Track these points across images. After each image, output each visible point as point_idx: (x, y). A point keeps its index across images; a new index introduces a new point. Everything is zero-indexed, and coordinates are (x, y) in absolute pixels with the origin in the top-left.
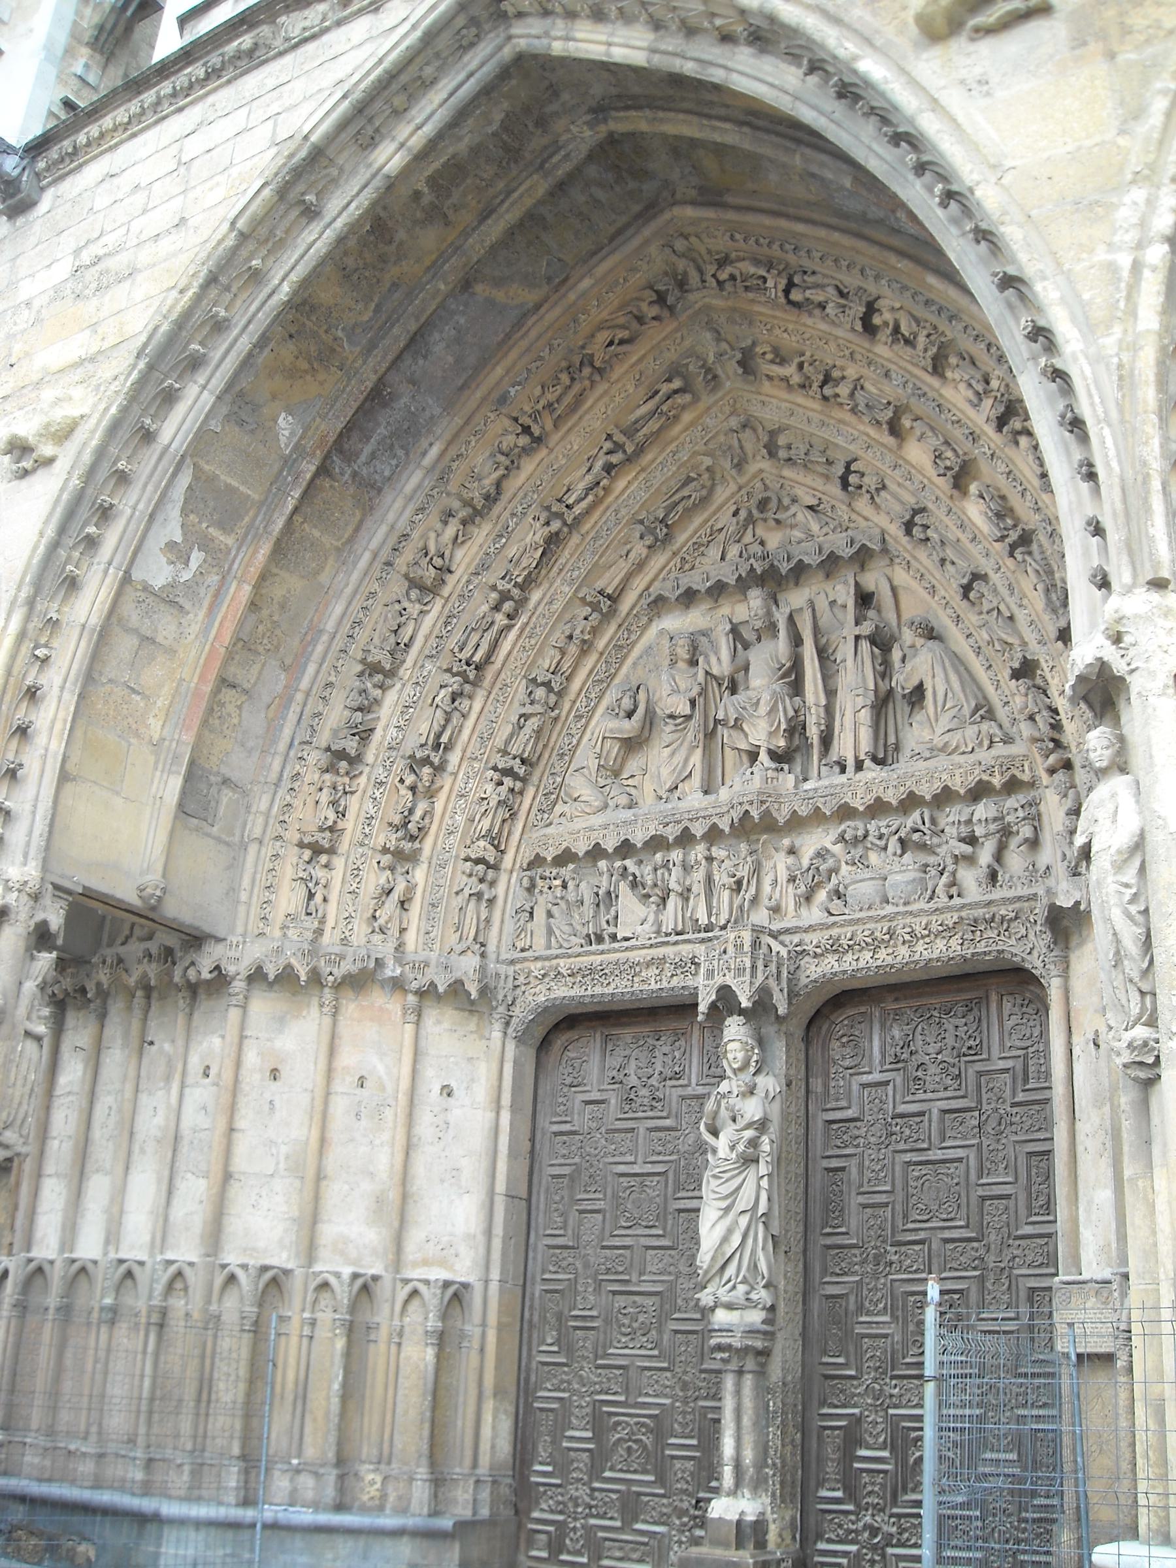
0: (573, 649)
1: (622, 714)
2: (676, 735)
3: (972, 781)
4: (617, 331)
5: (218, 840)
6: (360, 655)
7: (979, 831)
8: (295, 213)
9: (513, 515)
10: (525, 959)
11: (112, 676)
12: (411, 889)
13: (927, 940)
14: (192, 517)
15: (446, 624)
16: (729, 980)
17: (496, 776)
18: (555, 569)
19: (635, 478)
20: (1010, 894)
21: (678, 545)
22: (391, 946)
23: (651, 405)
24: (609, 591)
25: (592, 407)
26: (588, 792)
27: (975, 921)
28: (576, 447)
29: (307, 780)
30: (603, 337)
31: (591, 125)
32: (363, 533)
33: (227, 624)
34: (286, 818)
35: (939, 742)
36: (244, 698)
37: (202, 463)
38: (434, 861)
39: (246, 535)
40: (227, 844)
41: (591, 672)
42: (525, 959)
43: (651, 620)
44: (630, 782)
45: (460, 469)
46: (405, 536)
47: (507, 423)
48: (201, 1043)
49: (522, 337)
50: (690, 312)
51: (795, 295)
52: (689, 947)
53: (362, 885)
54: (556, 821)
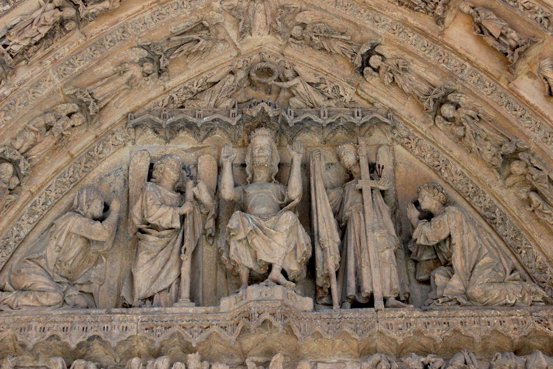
0: (49, 141)
26: (47, 281)
41: (57, 171)
44: (85, 288)
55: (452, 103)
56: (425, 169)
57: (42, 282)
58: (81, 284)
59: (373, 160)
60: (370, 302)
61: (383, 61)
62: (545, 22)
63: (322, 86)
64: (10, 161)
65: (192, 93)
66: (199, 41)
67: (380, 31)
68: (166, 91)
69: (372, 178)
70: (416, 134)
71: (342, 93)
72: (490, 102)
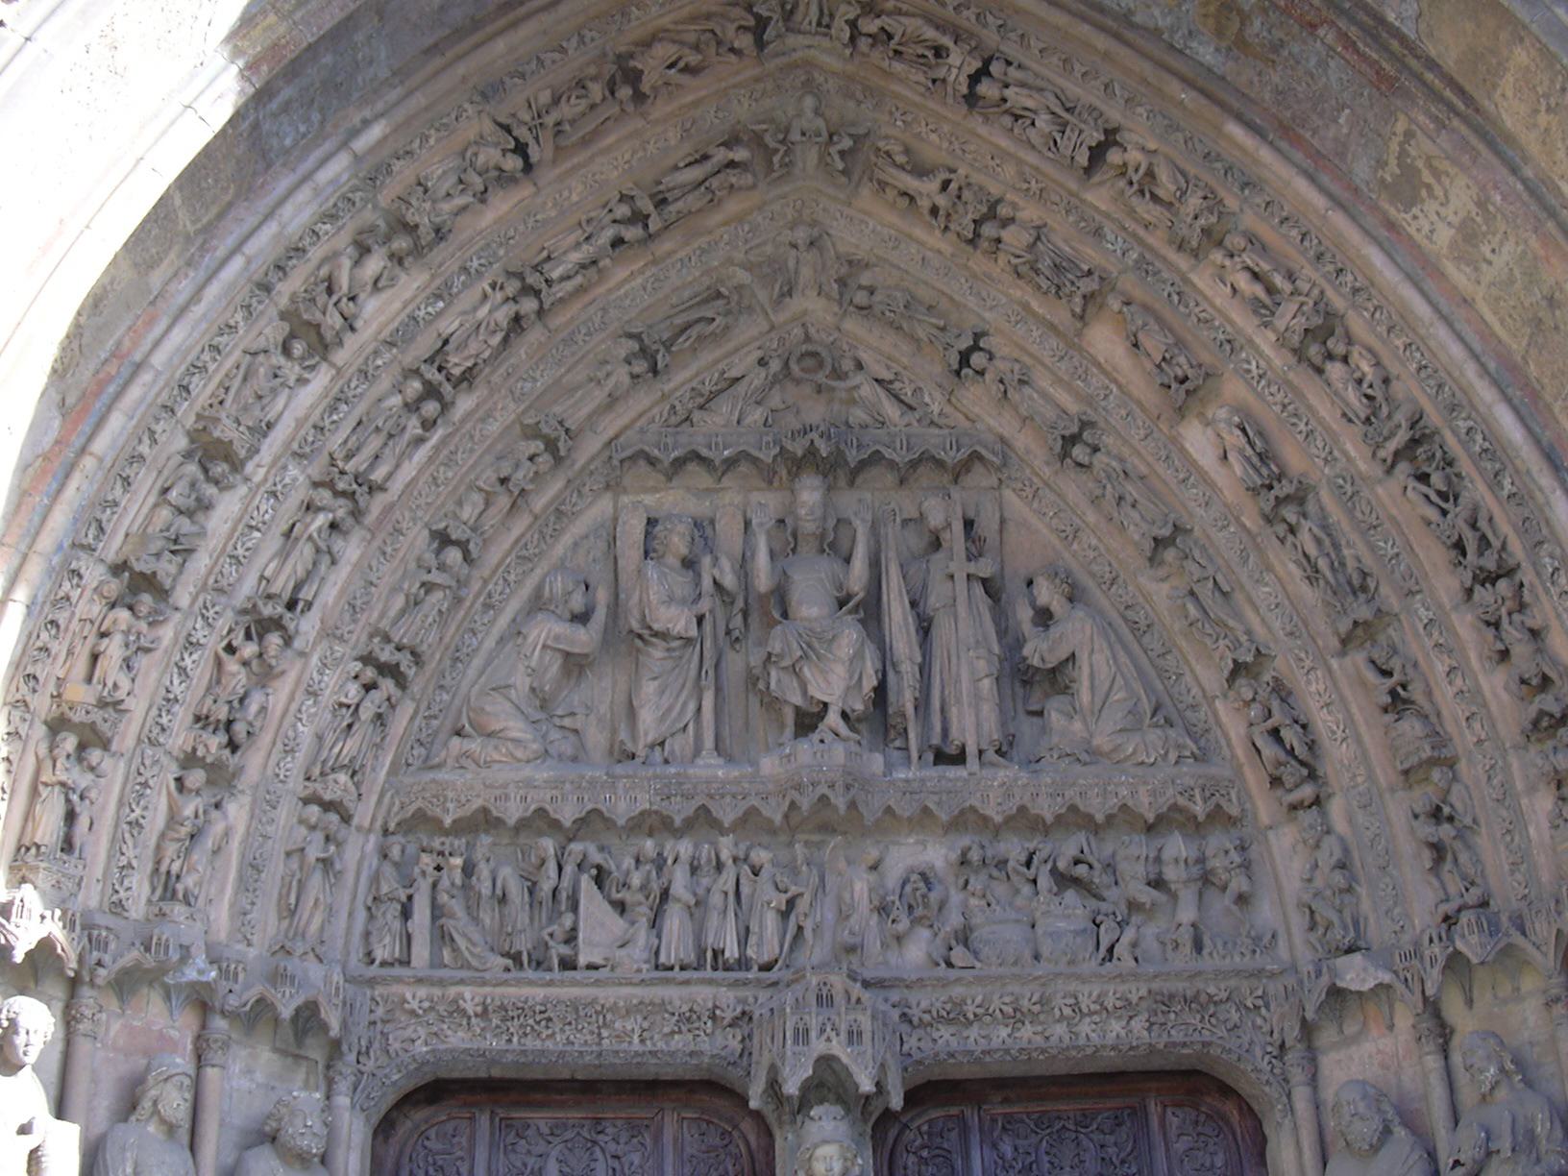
0: (503, 501)
1: (568, 616)
2: (670, 664)
3: (1163, 804)
4: (687, 51)
6: (190, 421)
7: (1171, 873)
9: (465, 269)
12: (227, 834)
13: (1096, 1018)
15: (333, 409)
16: (838, 1048)
17: (370, 673)
18: (502, 371)
19: (641, 272)
21: (672, 385)
23: (696, 173)
25: (608, 149)
26: (521, 725)
27: (1172, 996)
28: (575, 198)
29: (82, 610)
34: (37, 670)
41: (517, 541)
42: (399, 980)
44: (567, 722)
45: (405, 173)
46: (299, 251)
47: (488, 126)
50: (785, 60)
54: (450, 762)
55: (1087, 444)
56: (1045, 531)
57: (517, 728)
58: (561, 717)
59: (971, 514)
60: (959, 758)
61: (991, 359)
62: (1228, 347)
63: (897, 385)
64: (457, 543)
65: (702, 395)
66: (713, 320)
67: (987, 315)
69: (969, 560)
70: (1035, 480)
71: (927, 399)
72: (1143, 451)
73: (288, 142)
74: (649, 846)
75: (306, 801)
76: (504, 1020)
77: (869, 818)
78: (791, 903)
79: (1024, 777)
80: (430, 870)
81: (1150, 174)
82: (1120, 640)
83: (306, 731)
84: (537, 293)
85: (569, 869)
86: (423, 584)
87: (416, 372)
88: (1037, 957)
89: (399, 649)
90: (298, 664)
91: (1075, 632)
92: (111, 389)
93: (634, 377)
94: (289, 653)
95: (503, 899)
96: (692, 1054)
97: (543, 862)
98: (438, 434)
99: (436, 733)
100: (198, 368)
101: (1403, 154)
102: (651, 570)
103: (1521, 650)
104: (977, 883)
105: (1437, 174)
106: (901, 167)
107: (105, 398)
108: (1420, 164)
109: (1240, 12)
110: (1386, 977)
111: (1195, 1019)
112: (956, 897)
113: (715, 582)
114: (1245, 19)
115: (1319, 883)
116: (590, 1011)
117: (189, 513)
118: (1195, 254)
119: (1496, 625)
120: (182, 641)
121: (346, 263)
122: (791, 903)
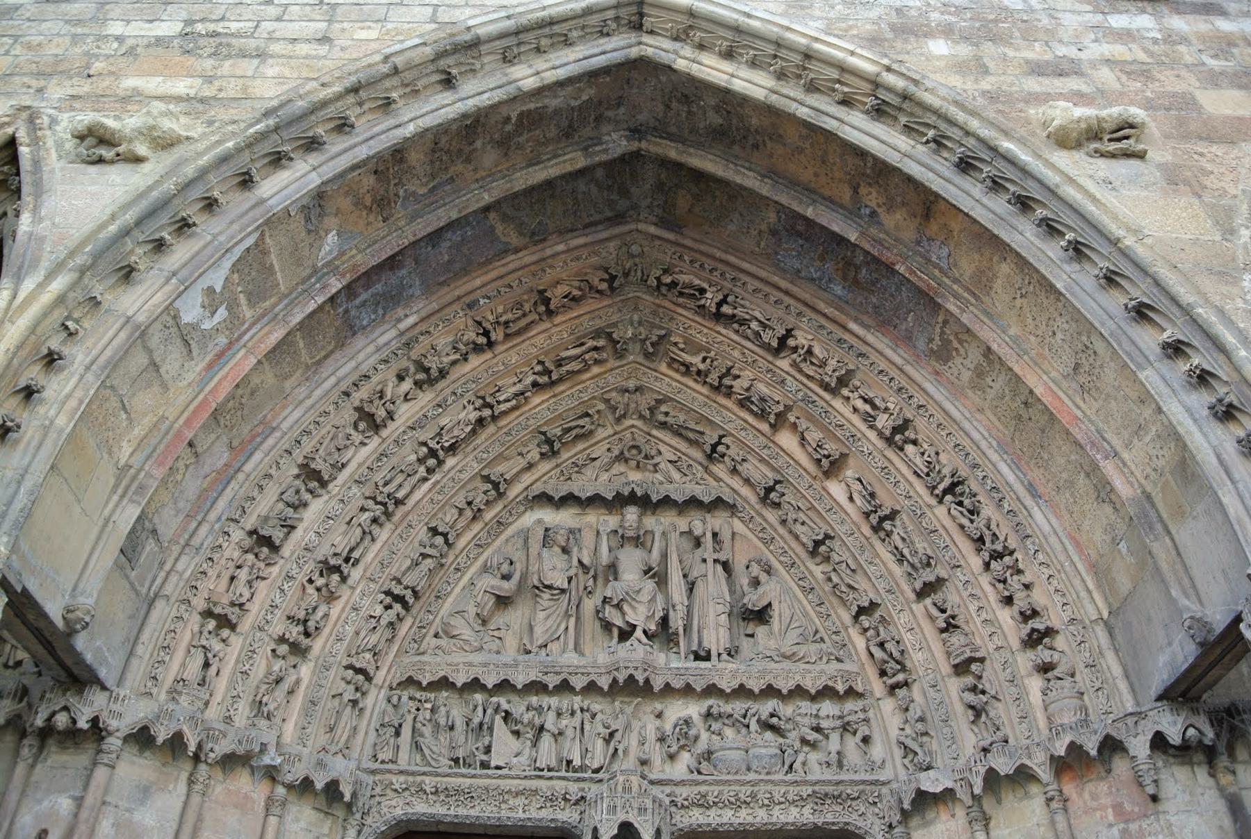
0: (469, 514)
2: (552, 603)
3: (820, 684)
5: (132, 584)
6: (300, 460)
7: (824, 724)
8: (437, 77)
10: (389, 771)
11: (115, 383)
12: (298, 682)
13: (783, 806)
14: (236, 276)
15: (379, 460)
16: (631, 818)
17: (388, 600)
18: (471, 447)
19: (547, 400)
20: (856, 777)
22: (275, 733)
24: (507, 477)
27: (826, 795)
29: (227, 554)
30: (562, 290)
31: (628, 139)
32: (330, 360)
33: (225, 383)
34: (198, 584)
35: (787, 650)
36: (193, 460)
37: (267, 234)
38: (320, 661)
39: (263, 316)
40: (136, 590)
42: (389, 771)
43: (526, 510)
44: (496, 633)
45: (425, 341)
46: (367, 377)
47: (470, 322)
48: (40, 802)
49: (503, 265)
51: (726, 309)
52: (563, 783)
53: (254, 669)
57: (467, 633)
59: (717, 530)
60: (707, 658)
68: (557, 466)
69: (715, 551)
73: (365, 323)
74: (534, 700)
75: (347, 668)
76: (447, 796)
77: (656, 689)
78: (612, 735)
79: (743, 667)
80: (413, 710)
81: (810, 352)
82: (795, 596)
83: (350, 630)
84: (491, 407)
85: (489, 711)
86: (421, 554)
87: (425, 444)
88: (749, 769)
89: (406, 588)
90: (348, 593)
91: (769, 591)
92: (258, 439)
93: (542, 454)
94: (344, 587)
95: (452, 728)
96: (552, 820)
97: (476, 707)
98: (435, 478)
99: (424, 636)
100: (307, 432)
101: (942, 333)
102: (545, 553)
103: (1020, 597)
104: (716, 726)
105: (961, 342)
106: (682, 350)
107: (254, 444)
108: (952, 337)
109: (855, 265)
110: (950, 785)
111: (839, 808)
112: (704, 736)
113: (580, 562)
114: (858, 269)
115: (908, 731)
116: (495, 793)
117: (295, 508)
118: (834, 391)
119: (1005, 581)
120: (284, 574)
121: (391, 385)
122: (612, 735)
